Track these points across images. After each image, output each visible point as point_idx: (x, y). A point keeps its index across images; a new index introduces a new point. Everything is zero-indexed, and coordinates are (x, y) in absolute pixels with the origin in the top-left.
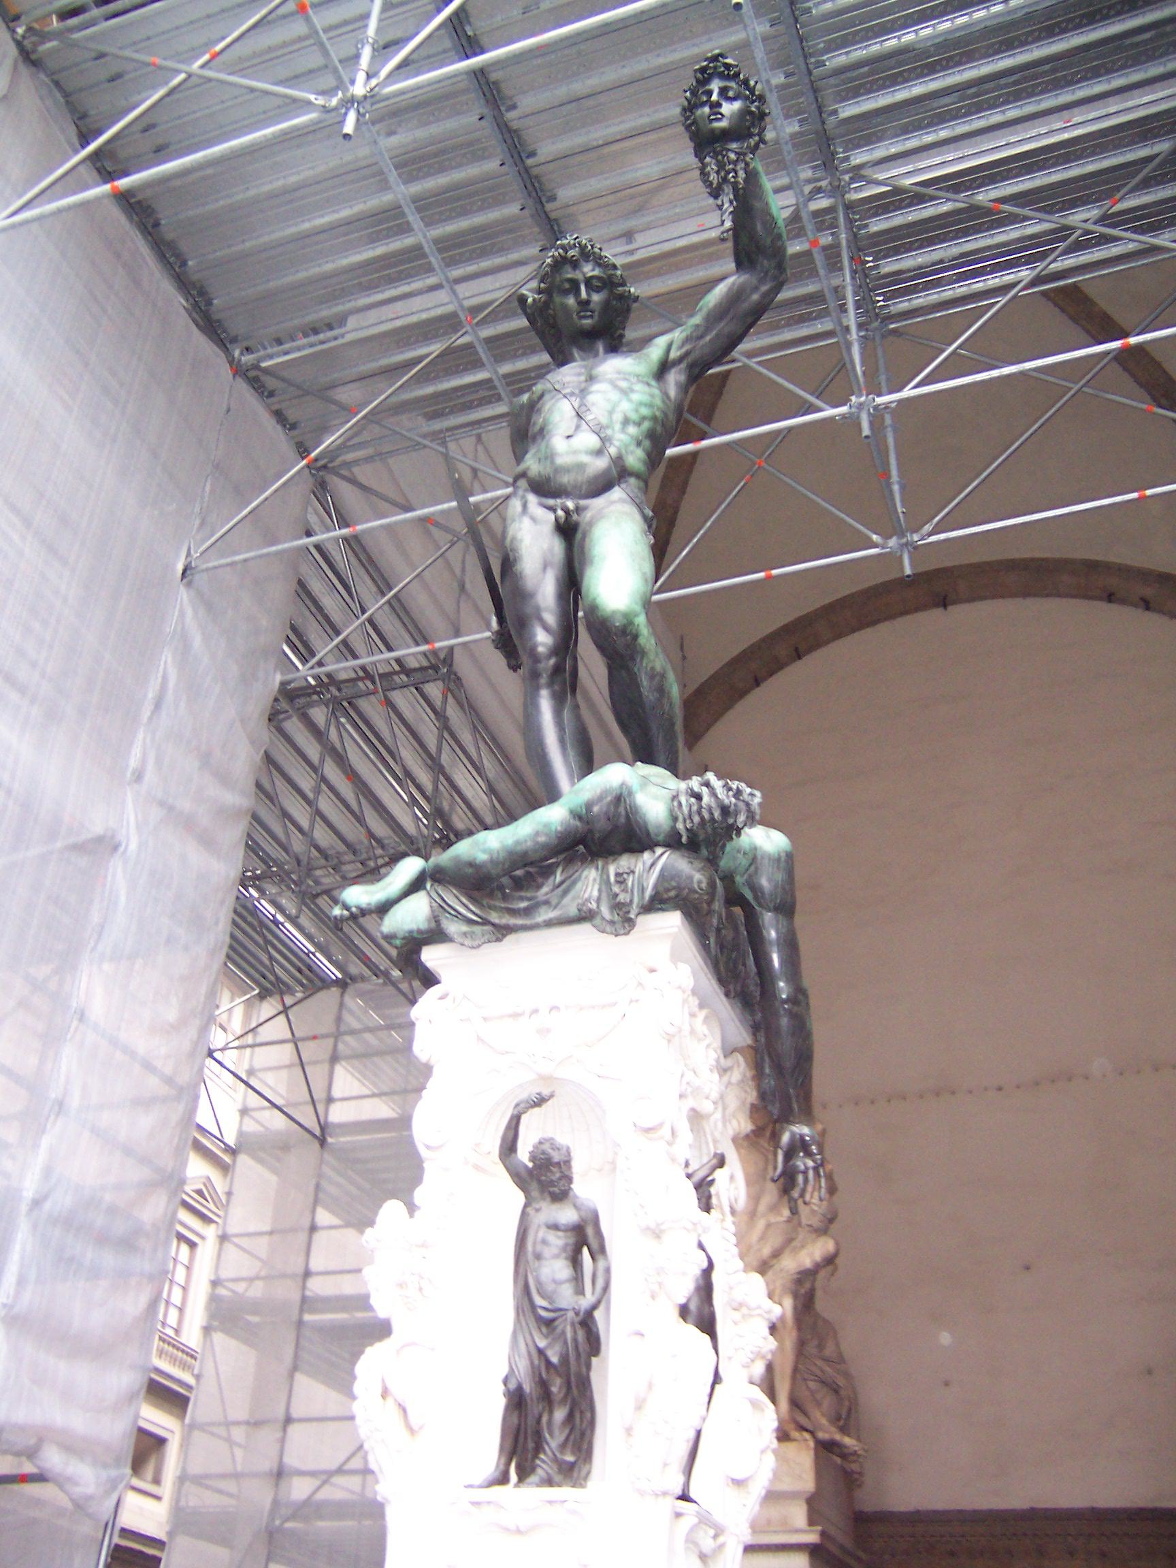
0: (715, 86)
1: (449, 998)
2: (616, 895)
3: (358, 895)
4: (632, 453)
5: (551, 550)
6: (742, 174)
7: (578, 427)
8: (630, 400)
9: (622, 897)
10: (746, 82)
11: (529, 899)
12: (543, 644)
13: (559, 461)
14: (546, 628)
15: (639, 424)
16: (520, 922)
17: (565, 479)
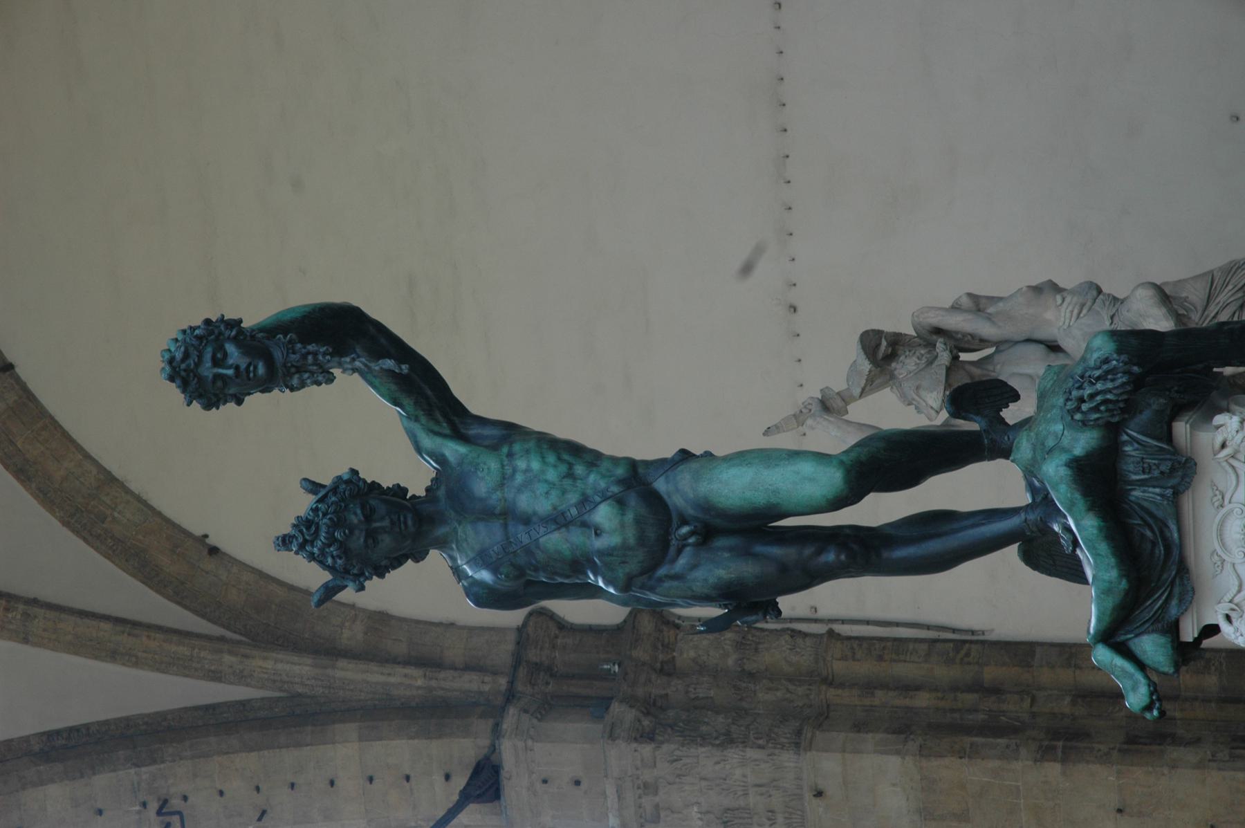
0: (207, 370)
1: (1233, 615)
2: (1162, 473)
3: (1136, 698)
4: (609, 470)
5: (730, 549)
6: (311, 348)
7: (585, 525)
8: (543, 472)
9: (1163, 468)
10: (199, 338)
11: (1154, 544)
12: (838, 556)
13: (632, 541)
14: (819, 552)
15: (571, 466)
16: (1176, 552)
17: (652, 534)
